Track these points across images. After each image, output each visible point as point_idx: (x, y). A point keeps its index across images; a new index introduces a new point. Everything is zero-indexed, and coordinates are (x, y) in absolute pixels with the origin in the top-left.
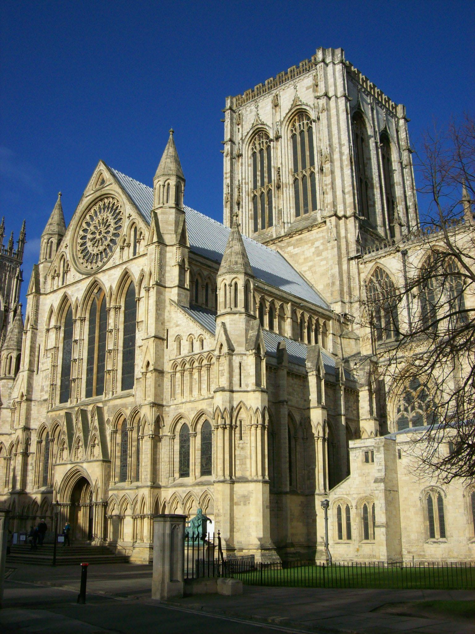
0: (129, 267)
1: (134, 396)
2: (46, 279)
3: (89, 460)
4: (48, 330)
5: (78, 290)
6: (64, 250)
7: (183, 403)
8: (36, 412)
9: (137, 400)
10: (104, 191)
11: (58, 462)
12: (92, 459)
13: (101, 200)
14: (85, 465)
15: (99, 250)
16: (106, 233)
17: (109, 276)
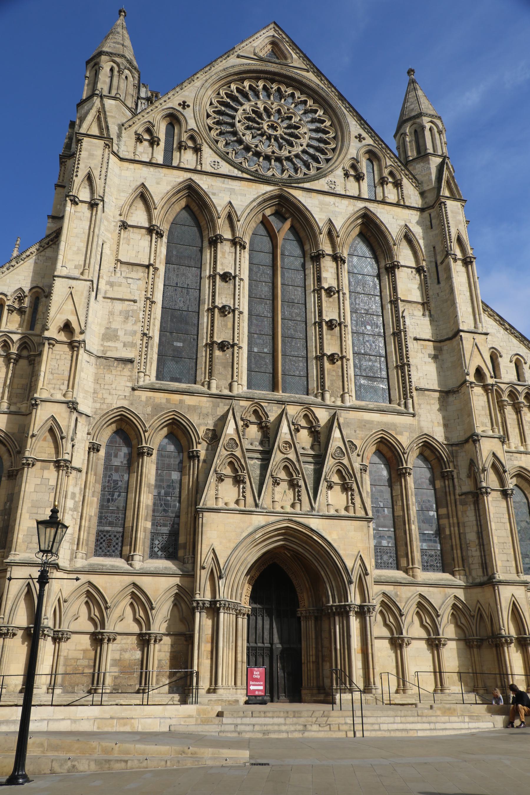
0: (371, 209)
1: (414, 415)
2: (120, 129)
3: (327, 513)
4: (124, 226)
5: (232, 191)
6: (180, 109)
7: (521, 453)
8: (91, 379)
9: (423, 424)
10: (284, 71)
11: (211, 503)
12: (332, 512)
13: (273, 81)
14: (314, 523)
15: (273, 152)
16: (285, 134)
17: (321, 203)
